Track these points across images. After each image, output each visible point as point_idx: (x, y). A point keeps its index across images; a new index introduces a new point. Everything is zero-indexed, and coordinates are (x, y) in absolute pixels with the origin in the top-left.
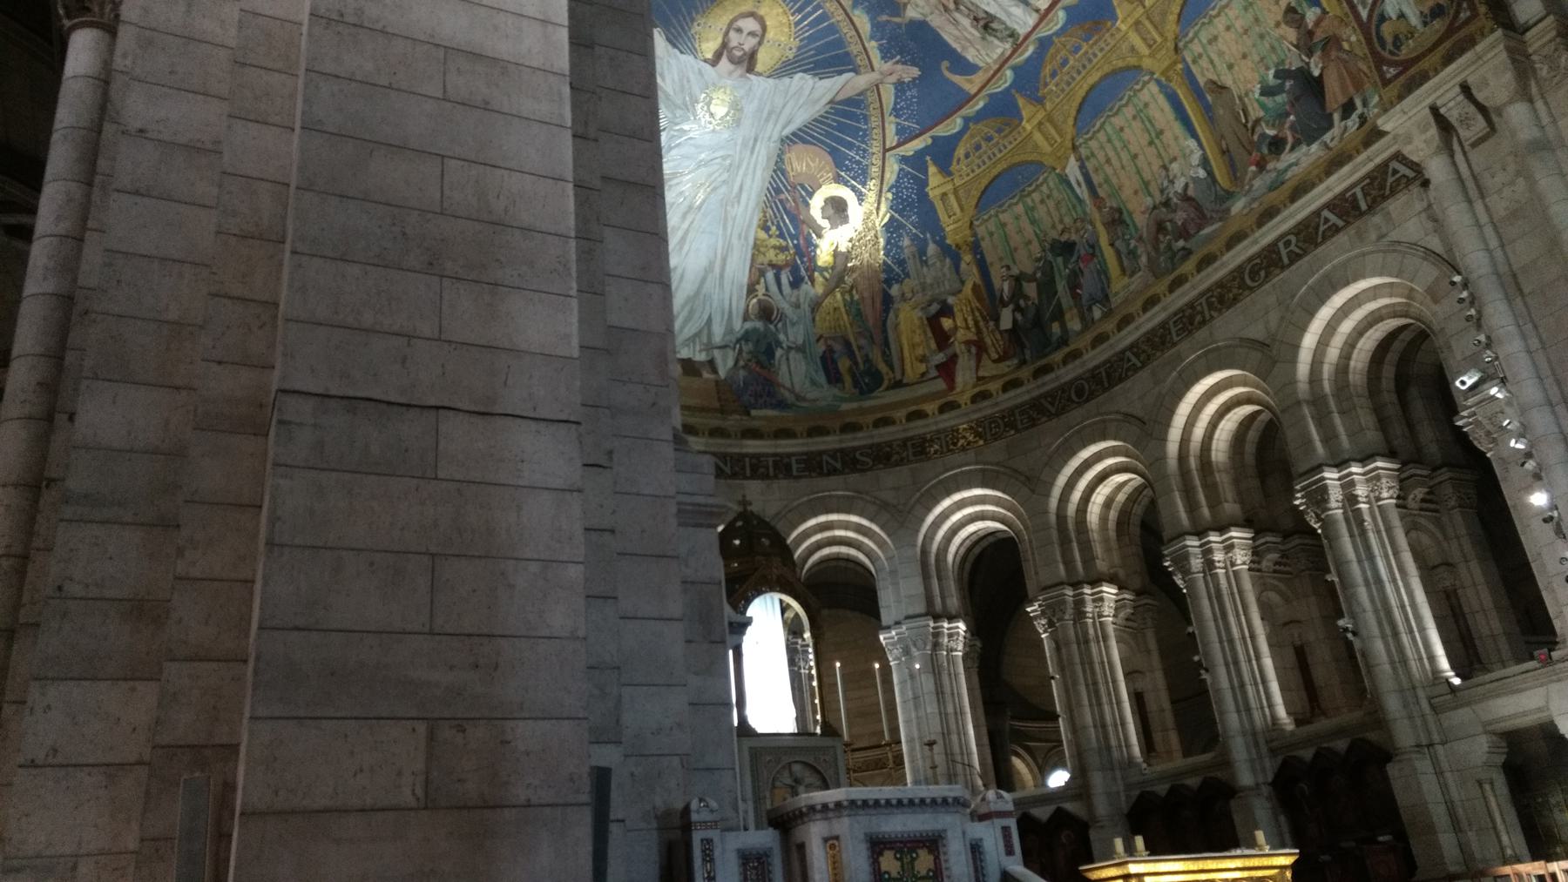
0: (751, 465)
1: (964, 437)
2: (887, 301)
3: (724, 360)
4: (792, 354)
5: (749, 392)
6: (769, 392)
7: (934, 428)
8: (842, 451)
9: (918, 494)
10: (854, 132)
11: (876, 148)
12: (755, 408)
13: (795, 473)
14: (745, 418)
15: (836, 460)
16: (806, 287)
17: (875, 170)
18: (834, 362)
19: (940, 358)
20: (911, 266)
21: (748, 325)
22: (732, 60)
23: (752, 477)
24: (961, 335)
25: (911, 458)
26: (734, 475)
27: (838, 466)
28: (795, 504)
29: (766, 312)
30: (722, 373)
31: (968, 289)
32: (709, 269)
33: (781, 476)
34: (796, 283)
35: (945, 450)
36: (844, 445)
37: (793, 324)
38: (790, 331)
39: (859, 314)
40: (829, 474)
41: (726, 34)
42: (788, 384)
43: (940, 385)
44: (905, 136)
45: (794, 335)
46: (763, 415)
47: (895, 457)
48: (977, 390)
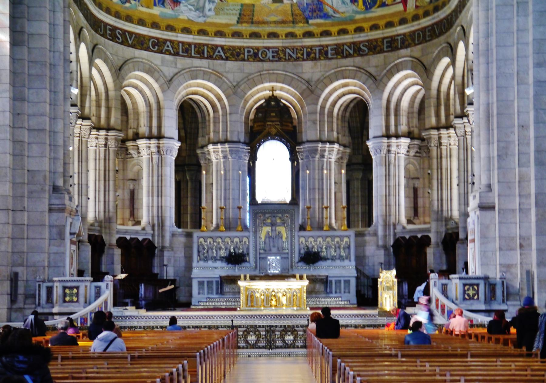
0: (307, 52)
1: (407, 40)
5: (309, 9)
6: (320, 8)
7: (395, 33)
8: (354, 43)
9: (385, 71)
12: (311, 19)
13: (330, 56)
14: (306, 25)
15: (351, 49)
23: (307, 60)
25: (385, 49)
26: (297, 59)
27: (351, 52)
28: (328, 74)
33: (322, 58)
35: (399, 46)
36: (355, 40)
40: (347, 57)
42: (330, 3)
43: (400, 7)
47: (378, 48)
48: (415, 13)
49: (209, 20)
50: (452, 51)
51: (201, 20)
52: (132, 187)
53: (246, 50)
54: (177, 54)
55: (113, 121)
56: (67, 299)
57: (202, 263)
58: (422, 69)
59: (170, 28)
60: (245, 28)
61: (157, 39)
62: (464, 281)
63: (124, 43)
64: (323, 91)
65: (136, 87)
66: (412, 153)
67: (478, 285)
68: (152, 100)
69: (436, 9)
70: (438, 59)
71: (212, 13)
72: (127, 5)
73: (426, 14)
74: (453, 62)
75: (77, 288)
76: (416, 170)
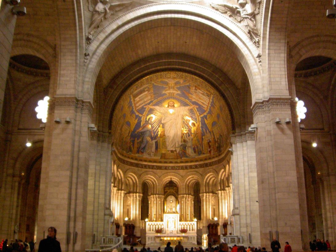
2: (203, 139)
3: (178, 149)
4: (189, 148)
10: (193, 113)
11: (196, 115)
13: (188, 168)
16: (190, 136)
17: (198, 119)
18: (195, 149)
19: (209, 150)
20: (205, 133)
21: (182, 143)
22: (170, 106)
23: (181, 170)
24: (212, 146)
26: (178, 169)
29: (185, 141)
30: (177, 152)
31: (212, 138)
32: (175, 135)
34: (189, 136)
37: (189, 143)
38: (188, 144)
39: (199, 141)
41: (168, 104)
42: (188, 153)
43: (209, 155)
44: (200, 115)
45: (189, 144)
46: (184, 159)
49: (152, 158)
50: (225, 167)
51: (150, 158)
52: (128, 208)
53: (163, 167)
54: (142, 168)
55: (123, 188)
56: (110, 242)
57: (149, 232)
58: (215, 172)
59: (141, 160)
60: (163, 160)
61: (137, 163)
62: (231, 237)
63: (127, 164)
64: (186, 179)
65: (130, 177)
66: (213, 198)
67: (235, 238)
68: (135, 182)
69: (219, 155)
70: (221, 169)
71: (153, 156)
72: (128, 153)
73: (216, 157)
74: (225, 171)
75: (113, 239)
76: (214, 203)
